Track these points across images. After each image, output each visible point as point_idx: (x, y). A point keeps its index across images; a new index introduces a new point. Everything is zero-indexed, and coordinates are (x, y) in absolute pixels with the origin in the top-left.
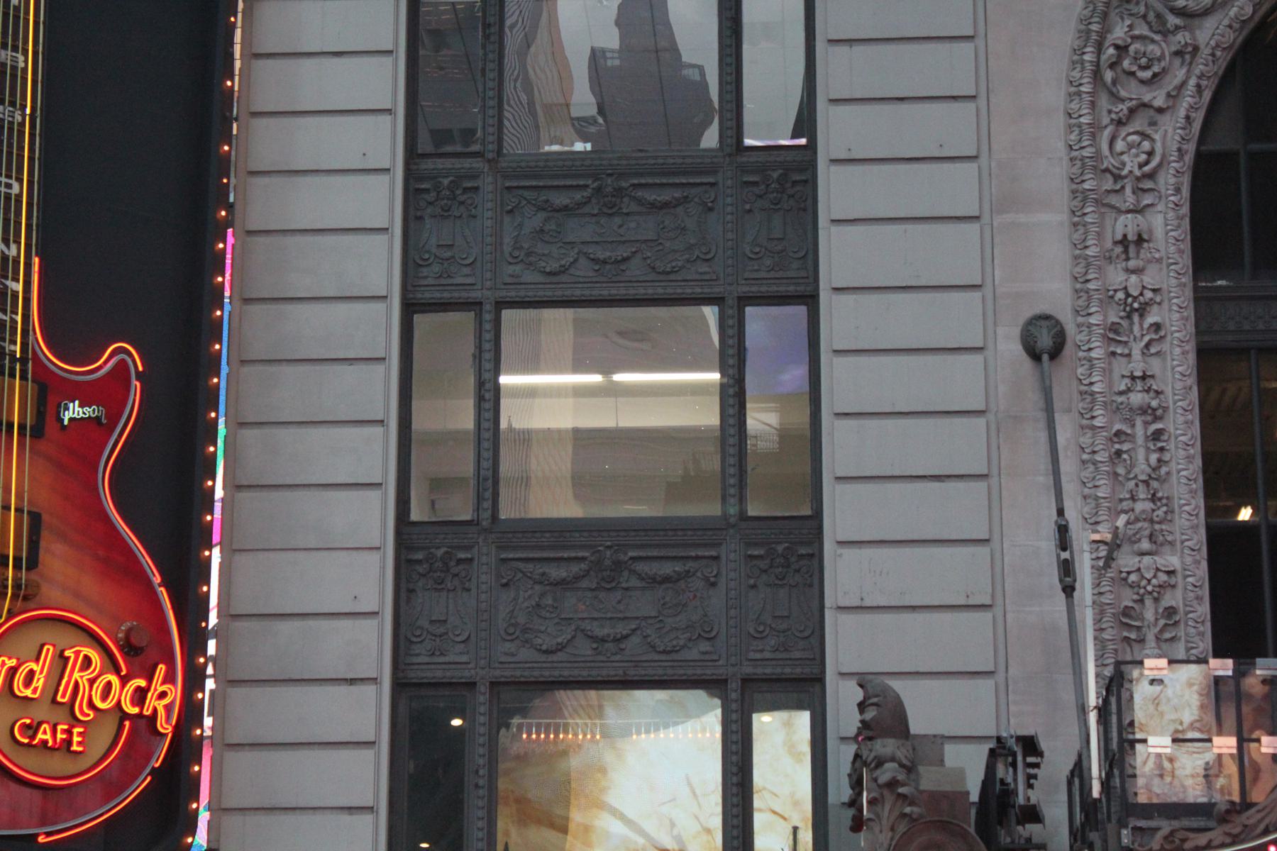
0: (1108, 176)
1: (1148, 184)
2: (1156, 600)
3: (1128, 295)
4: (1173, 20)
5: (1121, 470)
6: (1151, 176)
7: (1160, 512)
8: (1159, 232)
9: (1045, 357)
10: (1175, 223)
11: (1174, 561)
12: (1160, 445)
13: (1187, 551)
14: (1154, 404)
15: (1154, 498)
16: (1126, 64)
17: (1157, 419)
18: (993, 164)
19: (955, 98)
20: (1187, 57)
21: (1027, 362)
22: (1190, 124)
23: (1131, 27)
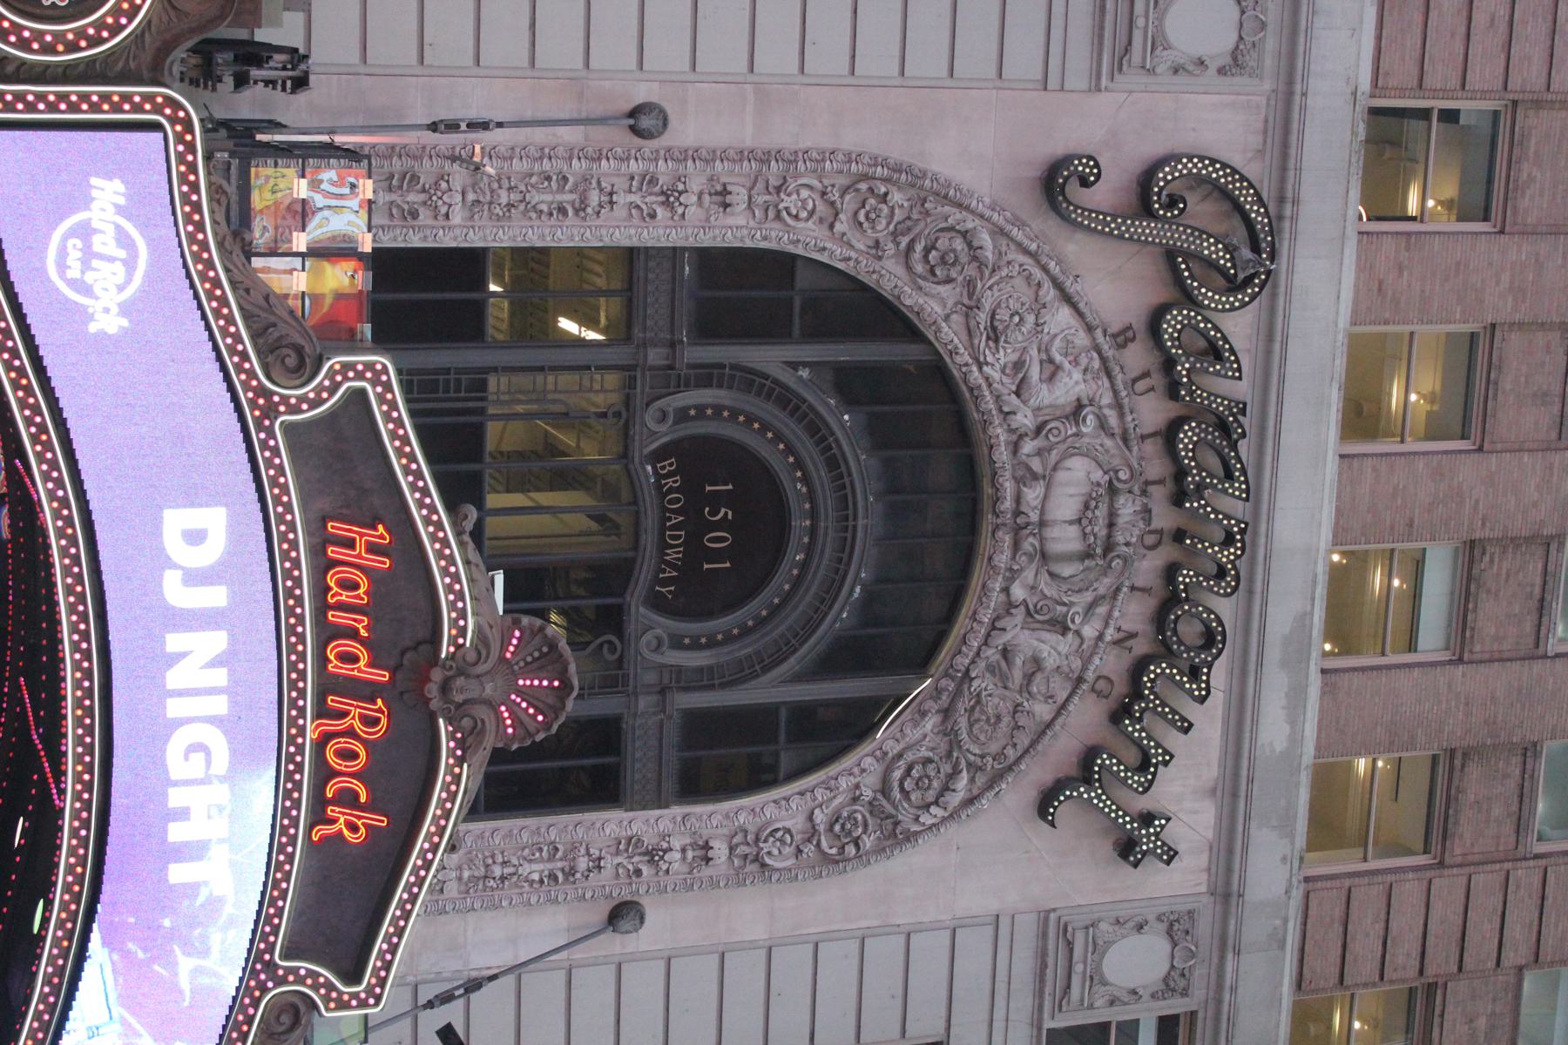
0: (781, 182)
1: (771, 214)
2: (425, 203)
3: (680, 193)
4: (904, 241)
5: (534, 180)
6: (778, 217)
7: (498, 210)
8: (730, 221)
9: (632, 122)
10: (739, 235)
11: (457, 218)
12: (555, 213)
13: (465, 231)
14: (589, 210)
15: (510, 205)
16: (872, 201)
17: (577, 212)
18: (796, 87)
19: (853, 57)
20: (874, 251)
21: (628, 107)
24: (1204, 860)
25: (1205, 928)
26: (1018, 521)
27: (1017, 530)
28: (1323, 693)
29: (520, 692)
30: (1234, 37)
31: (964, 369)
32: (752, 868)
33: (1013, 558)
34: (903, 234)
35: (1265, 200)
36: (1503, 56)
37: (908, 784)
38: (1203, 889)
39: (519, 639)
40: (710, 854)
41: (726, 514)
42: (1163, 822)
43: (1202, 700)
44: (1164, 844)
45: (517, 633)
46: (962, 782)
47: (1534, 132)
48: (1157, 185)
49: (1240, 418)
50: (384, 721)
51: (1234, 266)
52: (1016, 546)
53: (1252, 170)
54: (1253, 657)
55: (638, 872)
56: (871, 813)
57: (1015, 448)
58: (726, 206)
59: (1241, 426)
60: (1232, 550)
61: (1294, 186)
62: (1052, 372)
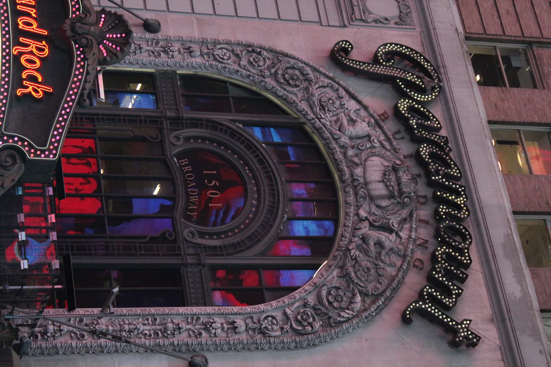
1: (211, 58)
3: (170, 47)
4: (273, 71)
8: (193, 60)
22: (235, 72)
23: (269, 58)
24: (498, 355)
26: (355, 184)
27: (355, 188)
28: (533, 278)
29: (109, 40)
30: (398, 11)
31: (312, 122)
32: (259, 337)
33: (357, 201)
34: (274, 67)
35: (429, 59)
36: (518, 25)
37: (330, 298)
39: (103, 22)
40: (236, 325)
41: (215, 183)
42: (468, 322)
44: (472, 333)
45: (103, 16)
46: (358, 298)
47: (544, 55)
50: (47, 50)
51: (423, 84)
52: (356, 194)
53: (419, 49)
54: (490, 253)
55: (200, 334)
56: (316, 314)
57: (345, 154)
58: (191, 52)
61: (441, 61)
62: (352, 122)
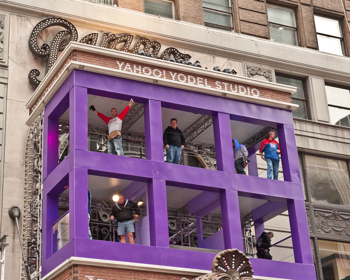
25: (251, 64)
28: (185, 20)
38: (241, 63)
43: (190, 57)
48: (39, 52)
49: (109, 35)
59: (111, 35)
60: (147, 43)
